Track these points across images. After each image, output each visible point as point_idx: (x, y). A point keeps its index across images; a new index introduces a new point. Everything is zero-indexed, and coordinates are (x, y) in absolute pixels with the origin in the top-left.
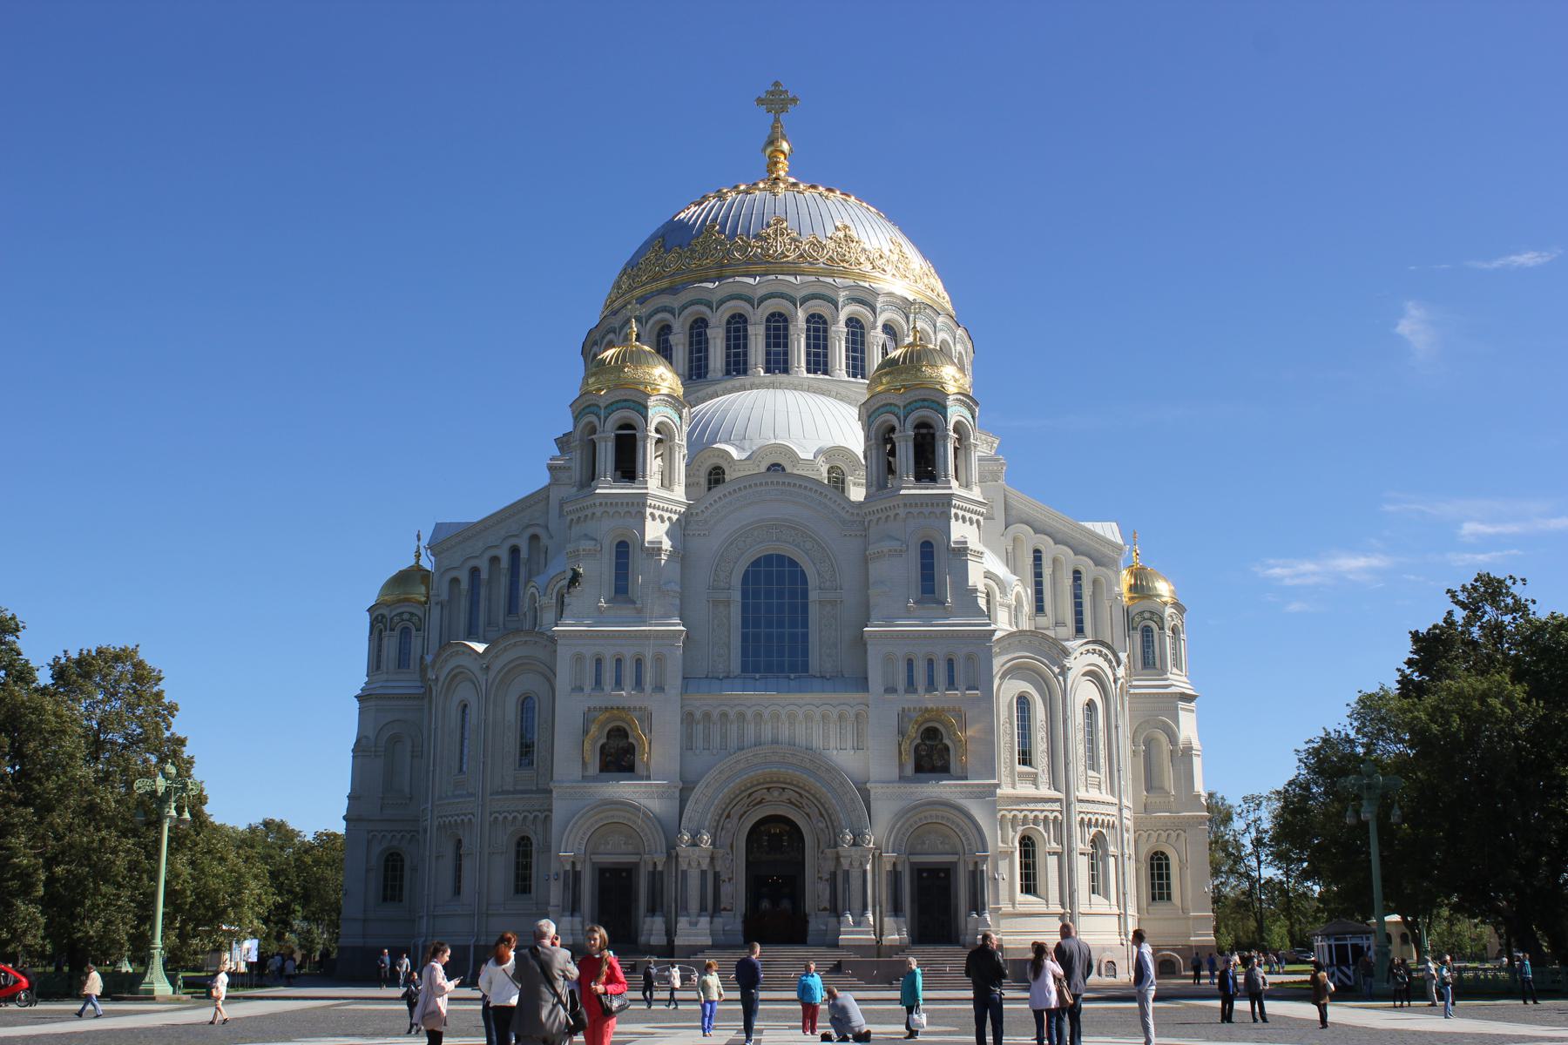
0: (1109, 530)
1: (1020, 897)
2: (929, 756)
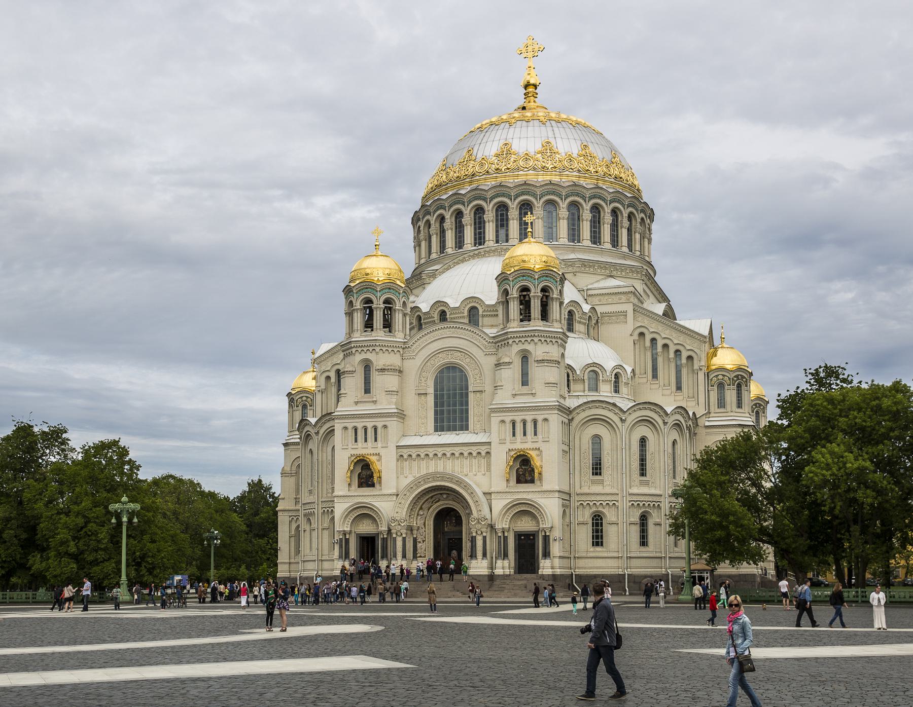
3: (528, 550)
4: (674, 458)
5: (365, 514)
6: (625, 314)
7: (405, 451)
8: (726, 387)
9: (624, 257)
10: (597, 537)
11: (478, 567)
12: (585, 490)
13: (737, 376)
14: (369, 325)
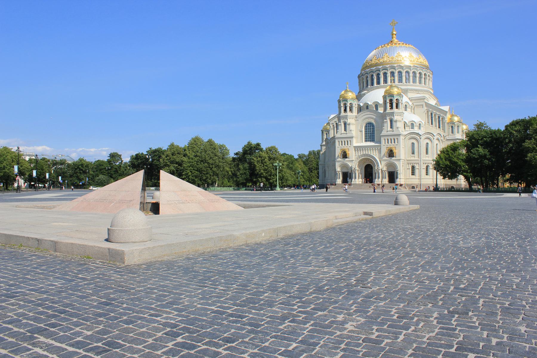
0: (446, 108)
3: (392, 177)
9: (423, 87)
11: (377, 181)
14: (345, 110)
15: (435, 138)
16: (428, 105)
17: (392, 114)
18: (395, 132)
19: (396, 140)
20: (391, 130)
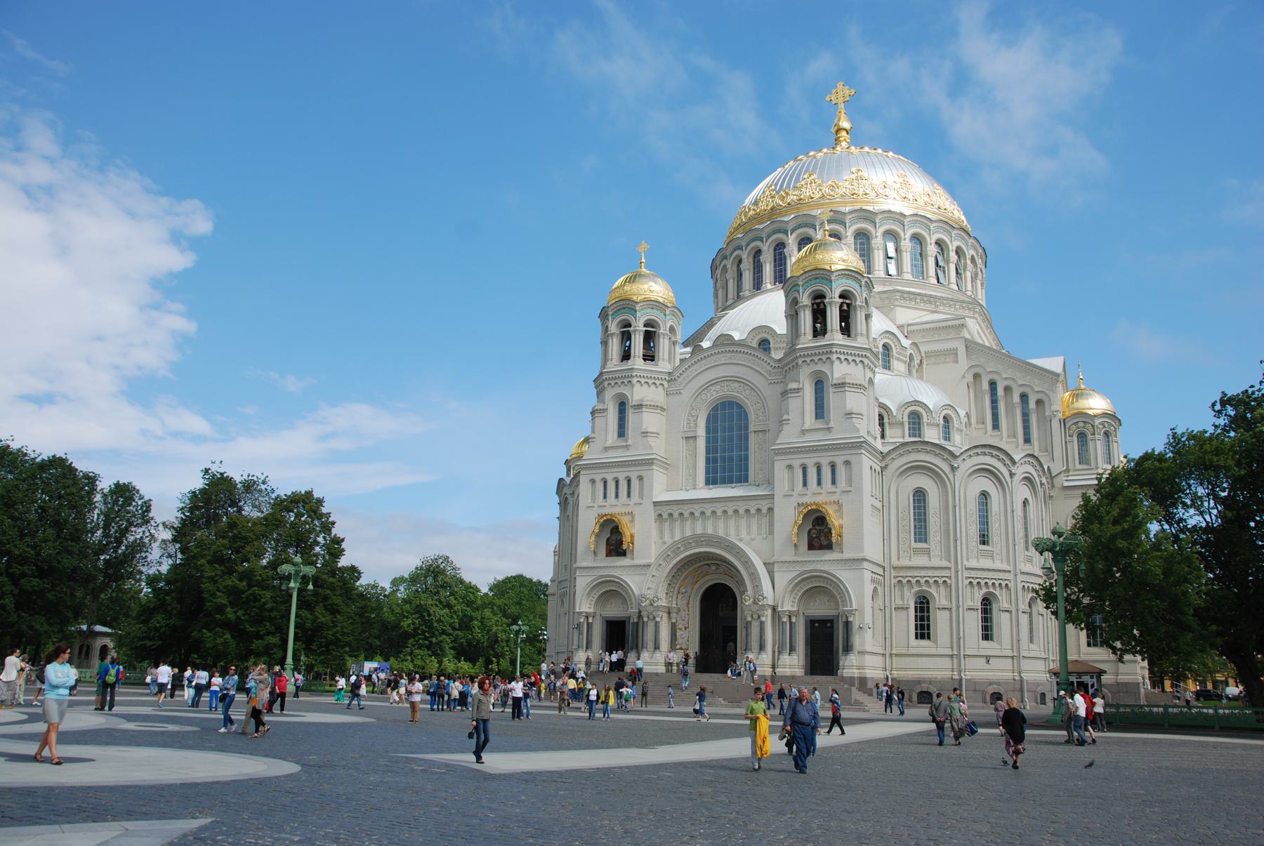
0: (1053, 364)
1: (985, 643)
2: (818, 538)
3: (825, 643)
4: (1026, 523)
5: (611, 591)
6: (954, 353)
7: (664, 508)
8: (1090, 437)
10: (922, 627)
12: (905, 562)
13: (1102, 423)
15: (1020, 471)
16: (970, 345)
17: (826, 354)
18: (840, 434)
19: (841, 472)
20: (819, 424)
